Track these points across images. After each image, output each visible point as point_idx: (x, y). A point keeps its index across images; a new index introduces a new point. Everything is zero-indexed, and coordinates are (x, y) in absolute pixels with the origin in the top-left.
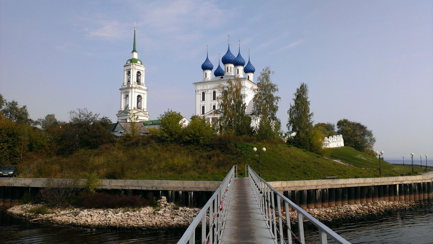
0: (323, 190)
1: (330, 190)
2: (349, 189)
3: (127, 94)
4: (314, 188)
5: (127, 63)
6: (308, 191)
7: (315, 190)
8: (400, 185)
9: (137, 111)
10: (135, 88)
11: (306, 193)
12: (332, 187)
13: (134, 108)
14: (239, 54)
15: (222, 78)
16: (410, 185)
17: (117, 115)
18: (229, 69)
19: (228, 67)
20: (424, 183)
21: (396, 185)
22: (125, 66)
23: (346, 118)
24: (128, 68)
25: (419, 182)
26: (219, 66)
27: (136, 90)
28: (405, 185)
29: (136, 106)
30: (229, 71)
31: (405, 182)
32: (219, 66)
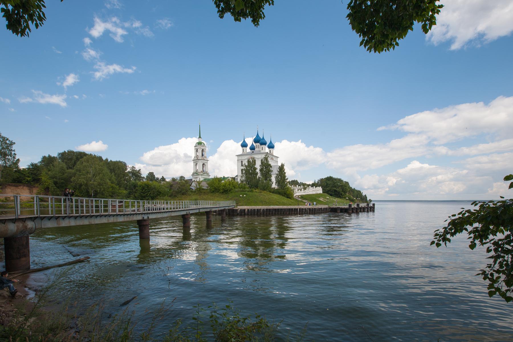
0: (264, 209)
1: (267, 209)
2: (275, 209)
3: (197, 163)
4: (260, 208)
5: (196, 145)
6: (257, 209)
7: (261, 209)
8: (300, 209)
9: (203, 173)
10: (201, 160)
11: (256, 210)
12: (267, 208)
13: (201, 171)
14: (263, 138)
15: (253, 152)
16: (305, 209)
17: (192, 175)
18: (258, 146)
19: (257, 145)
20: (312, 208)
21: (298, 209)
22: (195, 147)
23: (331, 176)
24: (197, 147)
25: (310, 208)
26: (253, 143)
27: (202, 161)
28: (303, 209)
29: (202, 170)
30: (258, 148)
31: (302, 208)
32: (253, 143)
